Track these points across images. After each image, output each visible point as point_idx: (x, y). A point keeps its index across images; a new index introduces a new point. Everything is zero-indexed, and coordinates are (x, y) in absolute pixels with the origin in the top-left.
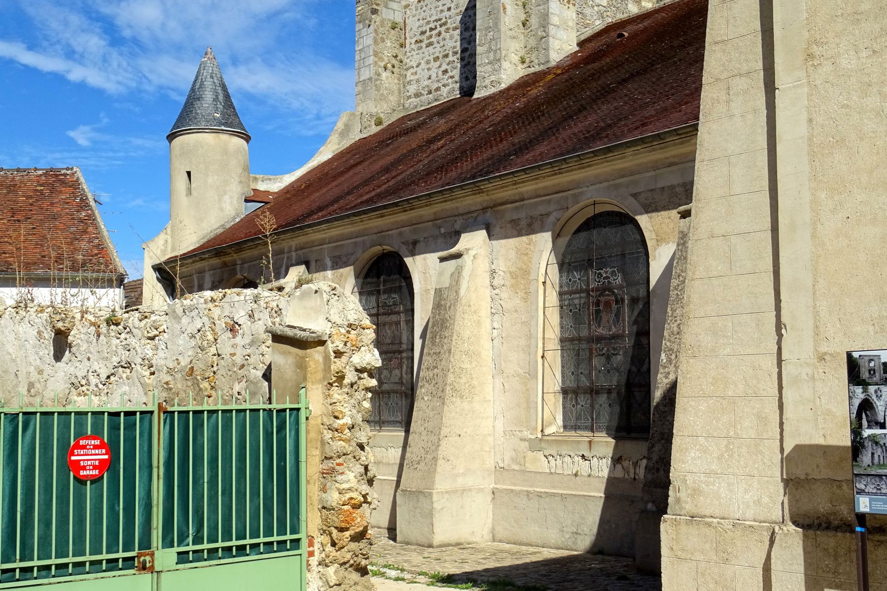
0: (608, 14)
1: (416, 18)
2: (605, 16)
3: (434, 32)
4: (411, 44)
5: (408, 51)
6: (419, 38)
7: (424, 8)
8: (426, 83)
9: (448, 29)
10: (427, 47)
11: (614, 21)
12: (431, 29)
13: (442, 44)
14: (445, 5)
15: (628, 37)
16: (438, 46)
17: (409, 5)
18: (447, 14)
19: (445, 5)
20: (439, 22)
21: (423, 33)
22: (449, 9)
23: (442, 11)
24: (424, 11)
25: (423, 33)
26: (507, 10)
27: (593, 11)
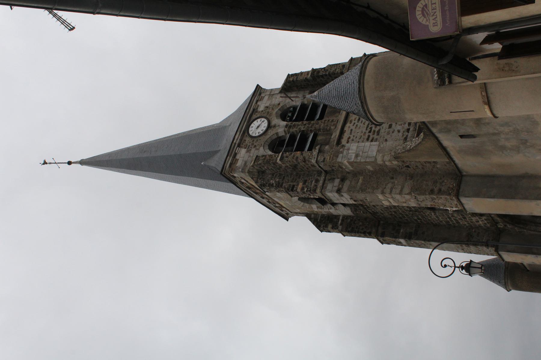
3: (373, 129)
8: (401, 134)
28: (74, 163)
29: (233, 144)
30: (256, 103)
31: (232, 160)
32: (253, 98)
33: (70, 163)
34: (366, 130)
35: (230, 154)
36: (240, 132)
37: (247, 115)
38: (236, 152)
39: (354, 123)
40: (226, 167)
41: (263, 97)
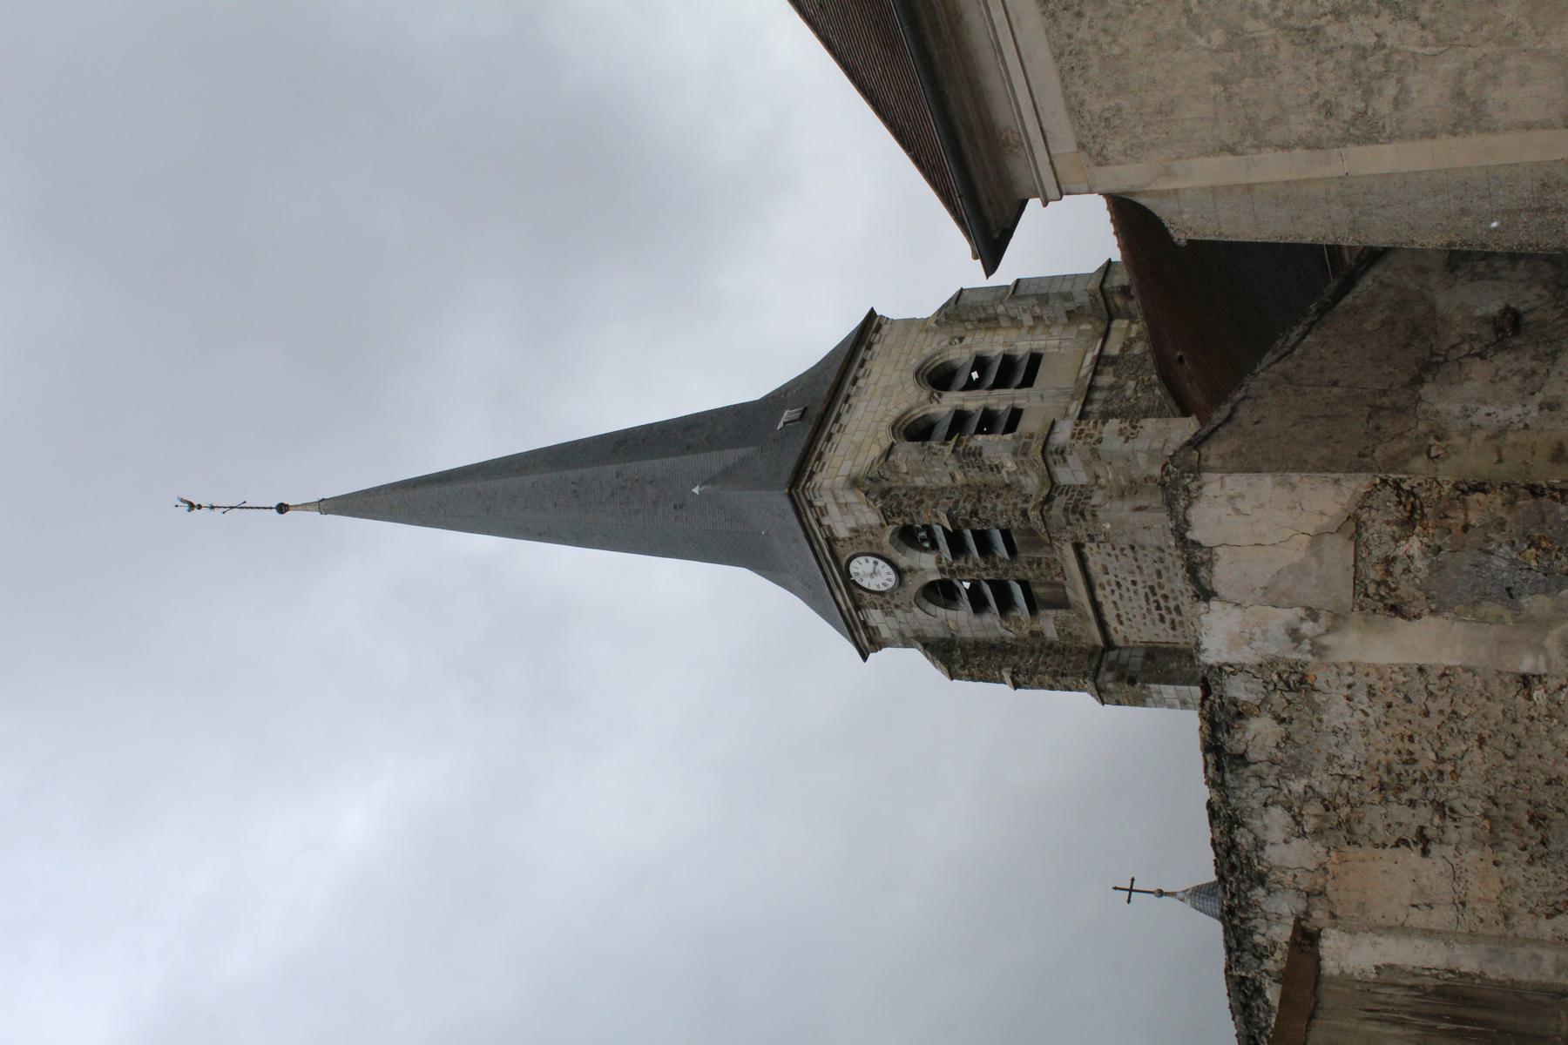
0: (1146, 379)
1: (1142, 627)
3: (1162, 603)
4: (1175, 636)
7: (1130, 616)
9: (1159, 584)
12: (1158, 608)
13: (1178, 594)
16: (1180, 598)
17: (1125, 637)
18: (1140, 585)
20: (1150, 596)
21: (1162, 619)
22: (1134, 583)
23: (1135, 592)
24: (1135, 616)
25: (1162, 619)
28: (296, 507)
29: (847, 614)
30: (820, 525)
31: (867, 633)
32: (805, 520)
33: (282, 508)
34: (1148, 604)
35: (854, 630)
37: (824, 554)
39: (1113, 591)
40: (862, 641)
41: (823, 509)
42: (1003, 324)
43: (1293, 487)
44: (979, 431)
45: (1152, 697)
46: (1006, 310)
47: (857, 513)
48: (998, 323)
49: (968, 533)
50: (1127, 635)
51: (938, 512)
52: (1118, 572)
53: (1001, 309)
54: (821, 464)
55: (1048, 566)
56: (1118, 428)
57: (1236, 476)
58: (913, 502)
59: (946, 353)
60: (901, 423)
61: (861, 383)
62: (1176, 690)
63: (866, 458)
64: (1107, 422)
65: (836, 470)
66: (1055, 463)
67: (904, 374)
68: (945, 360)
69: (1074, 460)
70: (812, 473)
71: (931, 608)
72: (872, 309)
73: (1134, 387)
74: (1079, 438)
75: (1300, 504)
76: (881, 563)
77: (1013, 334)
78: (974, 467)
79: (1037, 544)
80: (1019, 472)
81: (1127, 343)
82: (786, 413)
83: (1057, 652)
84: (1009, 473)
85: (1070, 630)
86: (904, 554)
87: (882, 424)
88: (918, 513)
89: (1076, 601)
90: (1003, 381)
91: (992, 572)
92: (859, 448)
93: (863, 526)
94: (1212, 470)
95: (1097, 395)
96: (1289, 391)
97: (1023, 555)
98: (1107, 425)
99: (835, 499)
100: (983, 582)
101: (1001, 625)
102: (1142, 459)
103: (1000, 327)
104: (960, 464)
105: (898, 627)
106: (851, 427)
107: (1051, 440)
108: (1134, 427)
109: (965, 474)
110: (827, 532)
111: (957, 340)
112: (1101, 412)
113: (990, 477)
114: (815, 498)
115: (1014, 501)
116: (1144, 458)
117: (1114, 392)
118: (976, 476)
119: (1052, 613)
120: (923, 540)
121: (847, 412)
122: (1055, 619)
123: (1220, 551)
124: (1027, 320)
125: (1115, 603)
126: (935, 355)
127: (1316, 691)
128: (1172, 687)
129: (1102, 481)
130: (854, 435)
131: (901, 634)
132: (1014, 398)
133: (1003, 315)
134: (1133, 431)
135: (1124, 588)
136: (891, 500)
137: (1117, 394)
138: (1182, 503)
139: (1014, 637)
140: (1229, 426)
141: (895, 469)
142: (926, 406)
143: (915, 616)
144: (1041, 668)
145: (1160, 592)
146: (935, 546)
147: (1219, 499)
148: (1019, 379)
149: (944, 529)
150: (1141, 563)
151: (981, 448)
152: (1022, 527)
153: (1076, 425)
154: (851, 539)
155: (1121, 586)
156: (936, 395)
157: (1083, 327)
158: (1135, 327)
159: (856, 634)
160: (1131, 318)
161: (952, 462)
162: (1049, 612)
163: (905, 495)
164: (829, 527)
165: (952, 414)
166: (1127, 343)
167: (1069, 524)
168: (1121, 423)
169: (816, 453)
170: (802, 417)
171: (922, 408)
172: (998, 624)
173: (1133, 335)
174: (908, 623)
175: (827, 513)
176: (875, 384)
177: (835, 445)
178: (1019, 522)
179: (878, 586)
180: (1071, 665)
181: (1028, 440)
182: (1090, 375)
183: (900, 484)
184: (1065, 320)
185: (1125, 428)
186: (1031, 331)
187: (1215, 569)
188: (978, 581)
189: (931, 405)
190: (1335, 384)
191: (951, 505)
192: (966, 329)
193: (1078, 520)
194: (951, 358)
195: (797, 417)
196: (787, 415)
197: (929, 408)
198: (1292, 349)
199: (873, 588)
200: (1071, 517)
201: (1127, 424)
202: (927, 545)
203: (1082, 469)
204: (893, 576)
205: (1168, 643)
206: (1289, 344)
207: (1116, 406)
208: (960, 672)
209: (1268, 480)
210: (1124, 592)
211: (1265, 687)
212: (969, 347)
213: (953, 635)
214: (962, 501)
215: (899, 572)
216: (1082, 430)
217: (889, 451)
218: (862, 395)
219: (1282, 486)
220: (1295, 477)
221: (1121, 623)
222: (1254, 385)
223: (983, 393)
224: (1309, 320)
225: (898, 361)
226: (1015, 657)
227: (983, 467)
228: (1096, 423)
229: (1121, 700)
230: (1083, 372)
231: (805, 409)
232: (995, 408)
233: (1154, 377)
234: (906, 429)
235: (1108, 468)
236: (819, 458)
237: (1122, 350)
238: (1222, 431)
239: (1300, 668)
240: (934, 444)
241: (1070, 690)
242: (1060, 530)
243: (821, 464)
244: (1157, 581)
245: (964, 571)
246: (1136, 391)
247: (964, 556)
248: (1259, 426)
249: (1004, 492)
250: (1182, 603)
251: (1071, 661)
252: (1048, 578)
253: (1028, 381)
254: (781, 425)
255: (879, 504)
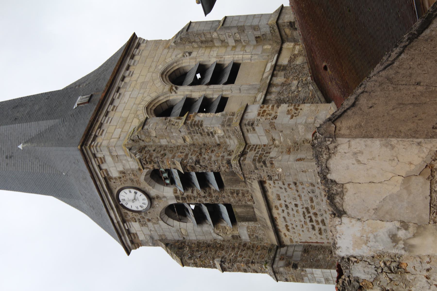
0: (304, 79)
2: (306, 82)
3: (314, 218)
4: (321, 238)
5: (327, 241)
6: (317, 231)
7: (294, 226)
9: (312, 207)
10: (324, 225)
11: (310, 75)
12: (311, 221)
13: (324, 212)
14: (292, 209)
15: (326, 62)
16: (325, 215)
17: (291, 239)
19: (292, 209)
20: (306, 214)
21: (313, 228)
22: (296, 205)
23: (297, 211)
25: (313, 228)
26: (302, 157)
27: (302, 91)
30: (100, 169)
32: (91, 166)
34: (305, 219)
35: (121, 234)
36: (112, 209)
37: (103, 188)
38: (127, 228)
39: (283, 211)
40: (127, 243)
41: (103, 159)
42: (216, 45)
43: (393, 147)
44: (201, 111)
45: (307, 276)
46: (218, 35)
47: (124, 162)
48: (213, 43)
49: (194, 174)
50: (292, 238)
51: (175, 161)
52: (286, 199)
53: (215, 35)
54: (101, 130)
55: (243, 195)
56: (287, 110)
57: (358, 140)
58: (159, 155)
59: (180, 62)
60: (152, 105)
61: (127, 80)
62: (323, 273)
63: (130, 127)
64: (280, 106)
65: (111, 134)
66: (248, 131)
67: (154, 75)
68: (180, 66)
69: (259, 129)
70: (96, 136)
71: (170, 221)
72: (134, 34)
73: (297, 84)
74: (263, 116)
75: (397, 158)
76: (139, 193)
77: (222, 51)
78: (197, 133)
79: (237, 181)
80: (225, 136)
81: (293, 57)
82: (79, 98)
83: (248, 248)
84: (219, 137)
85: (257, 235)
86: (154, 187)
87: (140, 106)
88: (163, 162)
89: (260, 217)
90: (215, 80)
91: (208, 199)
92: (125, 121)
93: (128, 170)
94: (343, 136)
95: (274, 89)
96: (391, 88)
97: (228, 188)
98: (280, 108)
99: (110, 153)
100: (203, 205)
101: (214, 232)
102: (301, 129)
103: (215, 46)
104: (189, 131)
105: (150, 233)
106: (120, 108)
107: (245, 117)
108: (297, 109)
109: (192, 138)
110: (105, 174)
111: (187, 54)
112: (276, 100)
113: (207, 140)
114: (97, 152)
115: (222, 154)
116: (302, 128)
117: (284, 88)
118: (199, 139)
119: (245, 224)
120: (166, 179)
121: (118, 98)
122: (248, 228)
123: (348, 186)
124: (231, 42)
125: (284, 218)
126: (173, 63)
127: (407, 273)
128: (320, 270)
129: (277, 142)
130: (122, 112)
131: (152, 238)
132: (223, 91)
133: (216, 38)
134: (296, 112)
135: (290, 208)
136: (145, 153)
137: (286, 89)
138: (325, 157)
139: (222, 239)
140: (354, 109)
141: (148, 135)
142: (168, 95)
143: (160, 226)
144: (239, 259)
145: (312, 211)
146: (173, 182)
147: (347, 155)
148: (226, 78)
149: (179, 171)
150: (300, 193)
151: (202, 121)
152: (227, 170)
153: (261, 108)
154: (120, 178)
155: (288, 207)
156: (174, 88)
157: (265, 47)
158: (297, 47)
159: (123, 238)
160: (295, 41)
161: (184, 130)
162: (243, 223)
163: (154, 151)
164: (106, 170)
165: (185, 100)
166: (293, 57)
167: (256, 169)
168: (289, 106)
169: (98, 124)
170: (89, 101)
171: (165, 96)
172: (212, 231)
173: (296, 52)
174: (156, 231)
175: (105, 162)
176: (136, 81)
177: (110, 119)
178: (225, 167)
179: (137, 208)
180: (257, 257)
181: (232, 117)
182: (270, 77)
183: (151, 143)
184: (255, 42)
185: (291, 110)
186: (234, 49)
187: (345, 197)
188: (200, 204)
189: (171, 94)
190: (418, 84)
191: (183, 157)
192: (193, 47)
193: (262, 166)
194: (184, 65)
195: (87, 101)
196: (79, 99)
197: (170, 96)
198: (393, 63)
199: (134, 208)
200: (257, 164)
201: (292, 107)
202: (168, 181)
203: (264, 135)
204: (146, 201)
205: (317, 242)
206: (391, 59)
207: (286, 96)
208: (189, 261)
209: (377, 143)
210: (290, 211)
211: (376, 270)
212: (195, 58)
213: (184, 238)
214: (190, 154)
215: (150, 199)
216: (265, 111)
217: (145, 123)
218: (128, 87)
219: (387, 146)
220: (394, 141)
221: (288, 230)
222: (369, 84)
223: (203, 87)
224: (403, 44)
225: (151, 66)
226: (223, 252)
227: (203, 133)
228: (273, 106)
229: (288, 278)
230: (266, 75)
231: (92, 96)
232: (211, 97)
233: (309, 78)
234: (155, 109)
235: (280, 134)
236: (100, 127)
237: (290, 62)
238: (349, 112)
239: (397, 259)
240: (173, 119)
241: (257, 272)
242: (251, 172)
243: (101, 130)
244: (310, 204)
245: (191, 198)
246: (298, 87)
247: (191, 189)
248: (372, 109)
249: (216, 149)
250: (326, 218)
251: (258, 254)
252: (243, 203)
253: (232, 80)
254: (76, 106)
255: (138, 156)
